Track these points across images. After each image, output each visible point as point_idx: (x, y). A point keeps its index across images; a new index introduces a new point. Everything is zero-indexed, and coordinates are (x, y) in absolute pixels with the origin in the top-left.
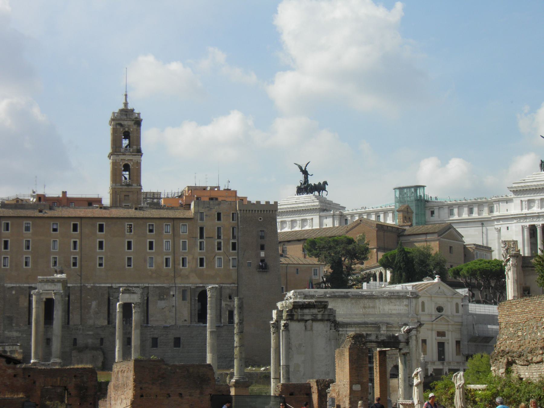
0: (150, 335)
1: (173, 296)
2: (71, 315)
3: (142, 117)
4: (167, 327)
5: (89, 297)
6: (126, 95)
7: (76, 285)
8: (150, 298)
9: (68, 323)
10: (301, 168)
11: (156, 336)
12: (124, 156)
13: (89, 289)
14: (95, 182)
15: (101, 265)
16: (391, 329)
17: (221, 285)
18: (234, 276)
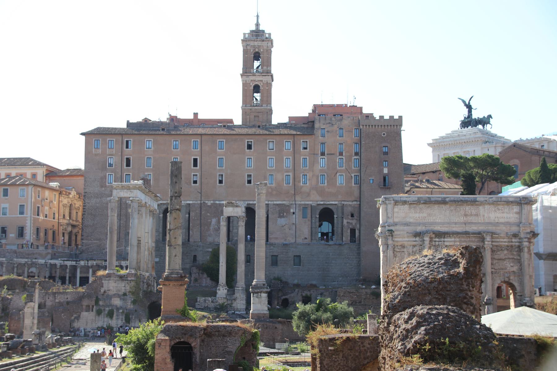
0: (270, 252)
1: (294, 213)
2: (191, 232)
3: (272, 37)
4: (286, 244)
5: (209, 214)
6: (258, 16)
7: (196, 202)
8: (269, 216)
9: (189, 240)
10: (464, 102)
11: (275, 254)
12: (254, 77)
13: (208, 206)
14: (226, 104)
15: (221, 182)
16: (498, 240)
17: (343, 202)
18: (356, 193)
